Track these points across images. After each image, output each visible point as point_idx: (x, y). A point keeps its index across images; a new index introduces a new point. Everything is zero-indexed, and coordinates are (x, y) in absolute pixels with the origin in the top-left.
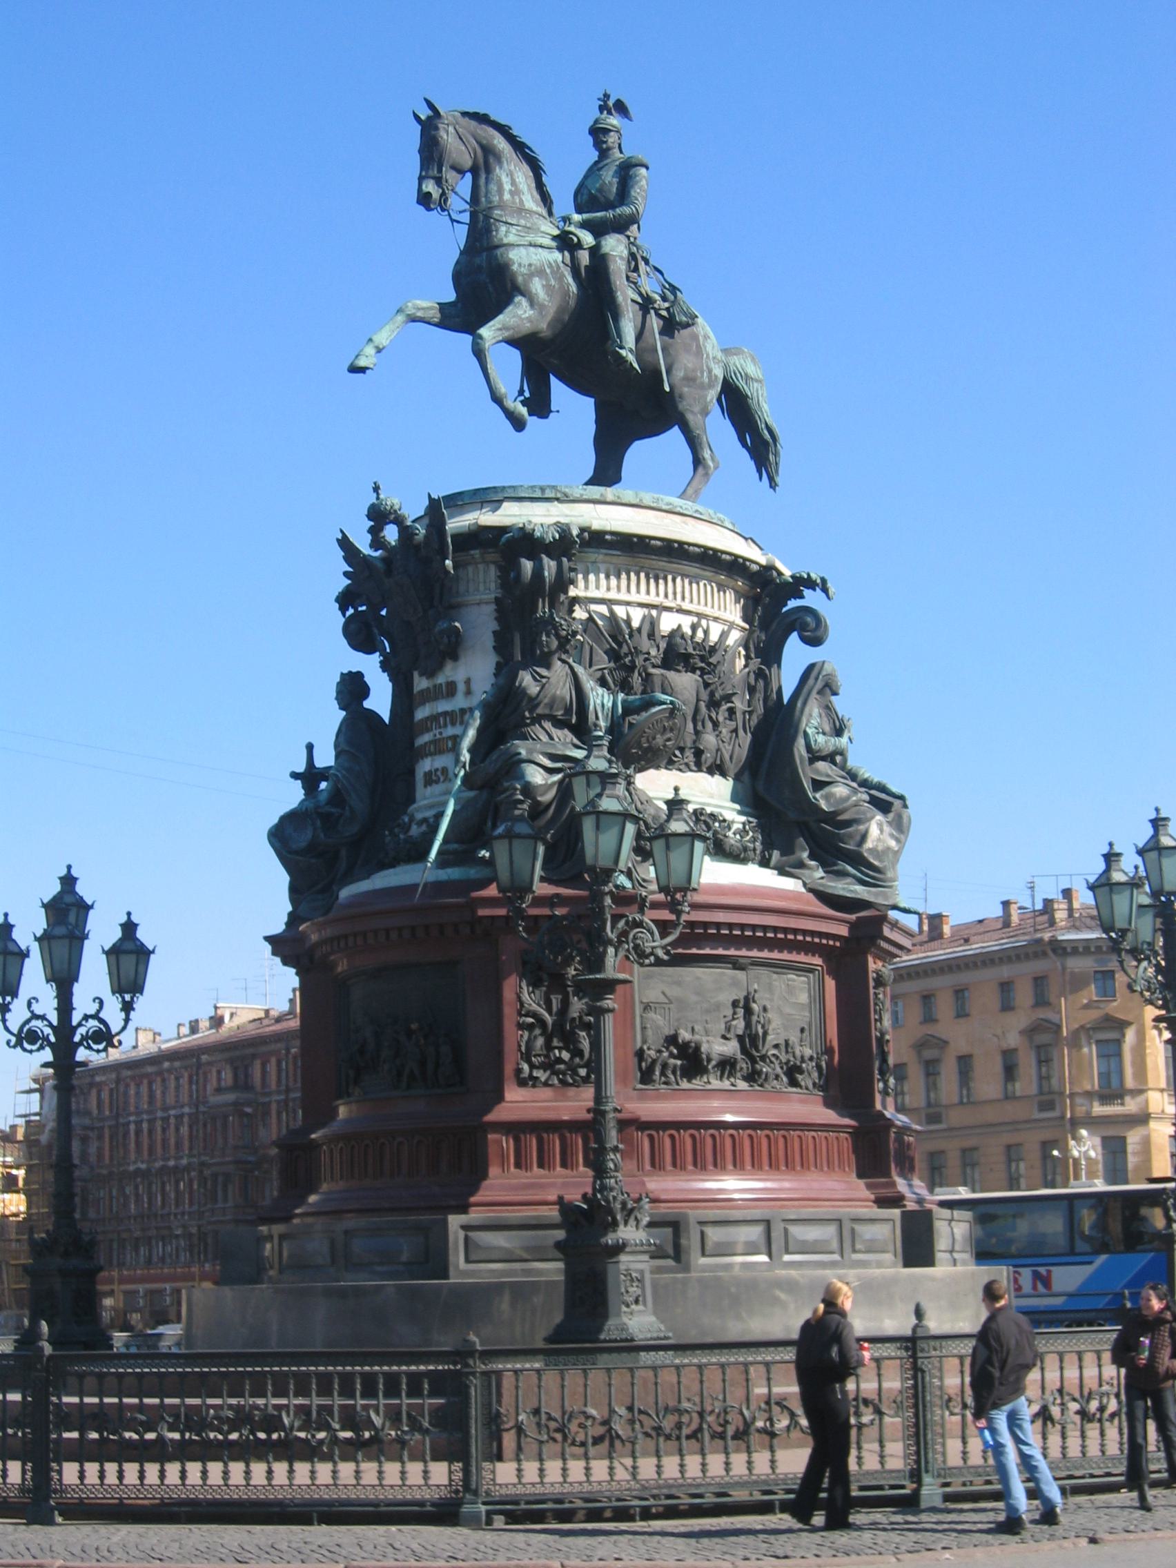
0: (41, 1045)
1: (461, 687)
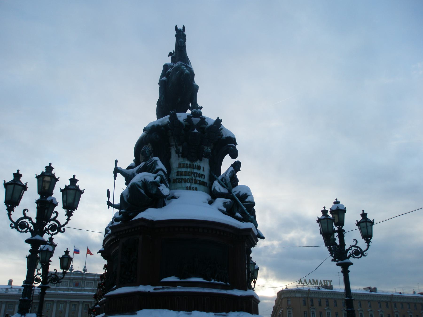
0: (27, 230)
1: (202, 169)
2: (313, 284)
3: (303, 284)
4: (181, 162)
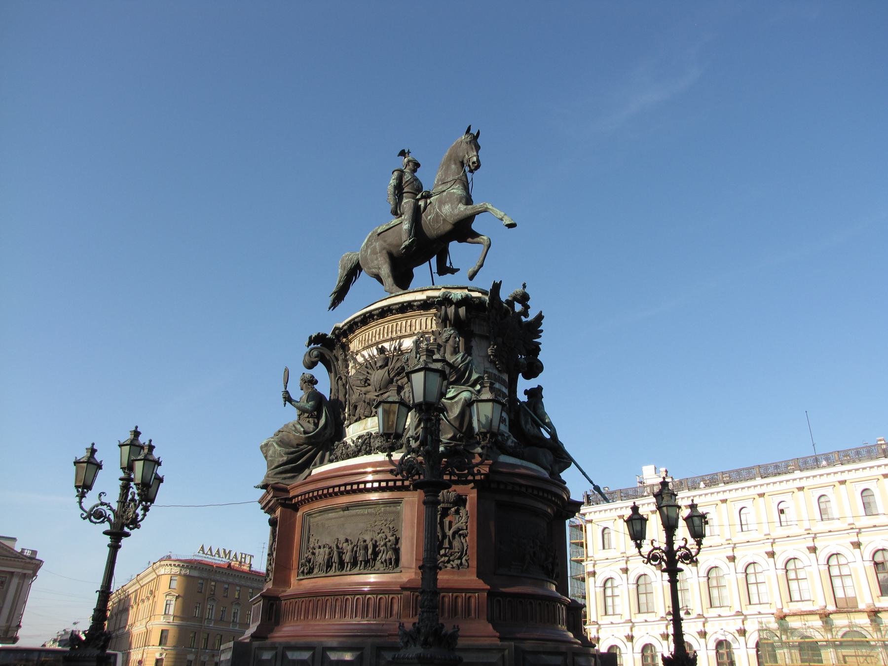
2: (223, 558)
3: (207, 554)
4: (487, 368)
